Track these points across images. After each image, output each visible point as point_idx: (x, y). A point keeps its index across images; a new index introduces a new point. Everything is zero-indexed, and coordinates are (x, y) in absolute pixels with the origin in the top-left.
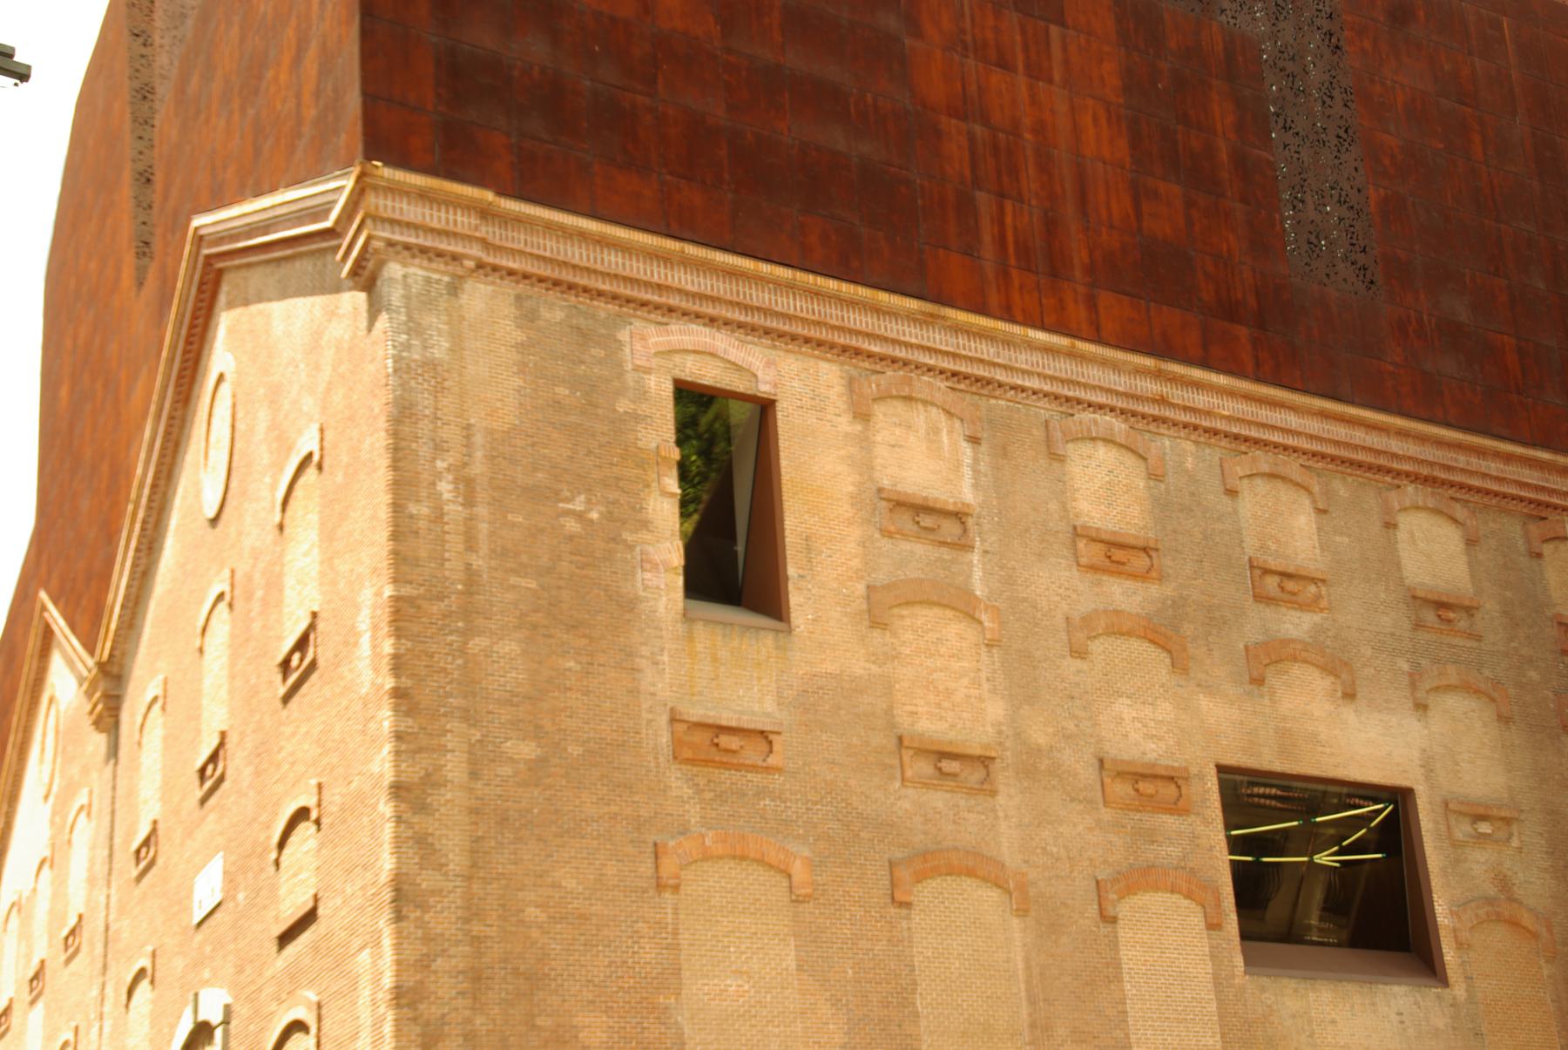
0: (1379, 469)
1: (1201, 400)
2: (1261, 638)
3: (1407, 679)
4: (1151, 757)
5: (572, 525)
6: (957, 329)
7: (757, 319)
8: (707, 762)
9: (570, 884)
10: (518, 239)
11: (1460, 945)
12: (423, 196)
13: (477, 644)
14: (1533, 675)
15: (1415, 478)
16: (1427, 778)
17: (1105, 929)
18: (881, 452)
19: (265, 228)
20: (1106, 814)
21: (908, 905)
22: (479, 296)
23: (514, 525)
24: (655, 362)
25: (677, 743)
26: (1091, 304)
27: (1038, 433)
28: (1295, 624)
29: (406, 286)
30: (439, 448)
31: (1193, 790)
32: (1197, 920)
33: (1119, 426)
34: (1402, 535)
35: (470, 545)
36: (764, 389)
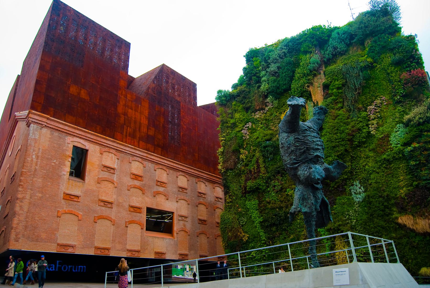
0: (177, 169)
1: (153, 157)
2: (156, 190)
3: (176, 198)
4: (137, 205)
5: (53, 164)
6: (118, 143)
7: (87, 138)
8: (68, 200)
9: (43, 215)
10: (52, 123)
11: (177, 233)
12: (39, 115)
13: (35, 179)
14: (194, 199)
15: (182, 171)
16: (177, 211)
17: (126, 228)
18: (104, 159)
19: (20, 117)
20: (129, 212)
21: (96, 222)
22: (45, 130)
23: (44, 163)
24: (70, 143)
25: (64, 196)
26: (139, 143)
27: (128, 159)
28: (161, 189)
29: (33, 127)
30: (34, 151)
31: (142, 210)
32: (140, 228)
33: (140, 160)
34: (179, 178)
35: (36, 165)
36: (87, 148)
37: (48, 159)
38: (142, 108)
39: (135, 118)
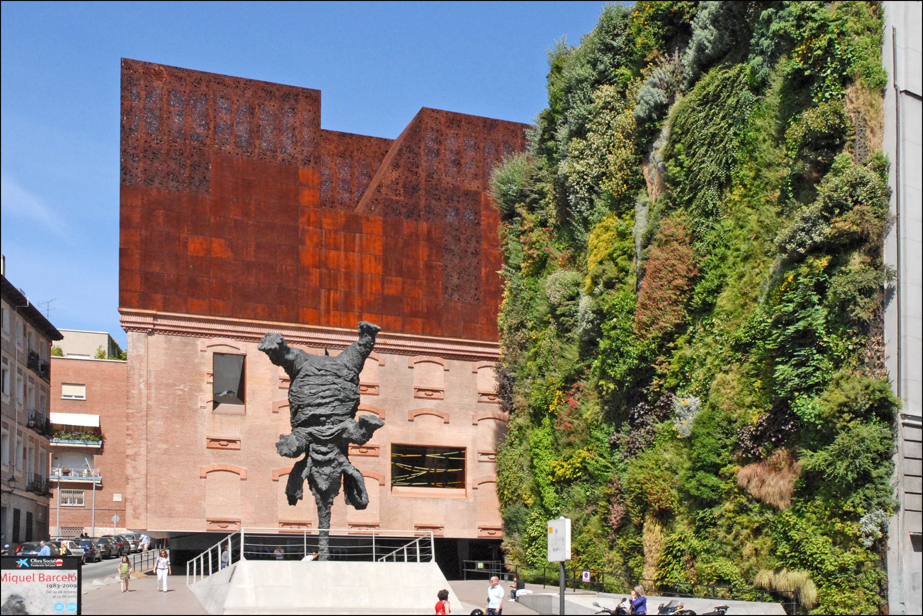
5: (179, 392)
22: (157, 338)
30: (140, 376)
37: (167, 385)
38: (364, 239)
39: (347, 267)
